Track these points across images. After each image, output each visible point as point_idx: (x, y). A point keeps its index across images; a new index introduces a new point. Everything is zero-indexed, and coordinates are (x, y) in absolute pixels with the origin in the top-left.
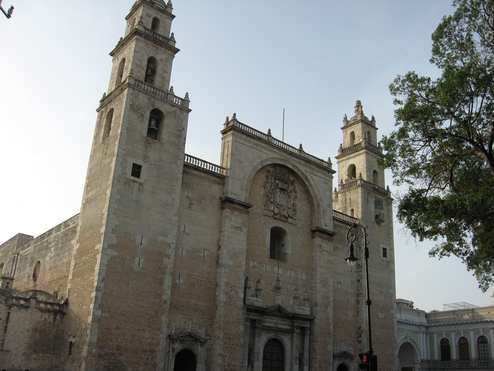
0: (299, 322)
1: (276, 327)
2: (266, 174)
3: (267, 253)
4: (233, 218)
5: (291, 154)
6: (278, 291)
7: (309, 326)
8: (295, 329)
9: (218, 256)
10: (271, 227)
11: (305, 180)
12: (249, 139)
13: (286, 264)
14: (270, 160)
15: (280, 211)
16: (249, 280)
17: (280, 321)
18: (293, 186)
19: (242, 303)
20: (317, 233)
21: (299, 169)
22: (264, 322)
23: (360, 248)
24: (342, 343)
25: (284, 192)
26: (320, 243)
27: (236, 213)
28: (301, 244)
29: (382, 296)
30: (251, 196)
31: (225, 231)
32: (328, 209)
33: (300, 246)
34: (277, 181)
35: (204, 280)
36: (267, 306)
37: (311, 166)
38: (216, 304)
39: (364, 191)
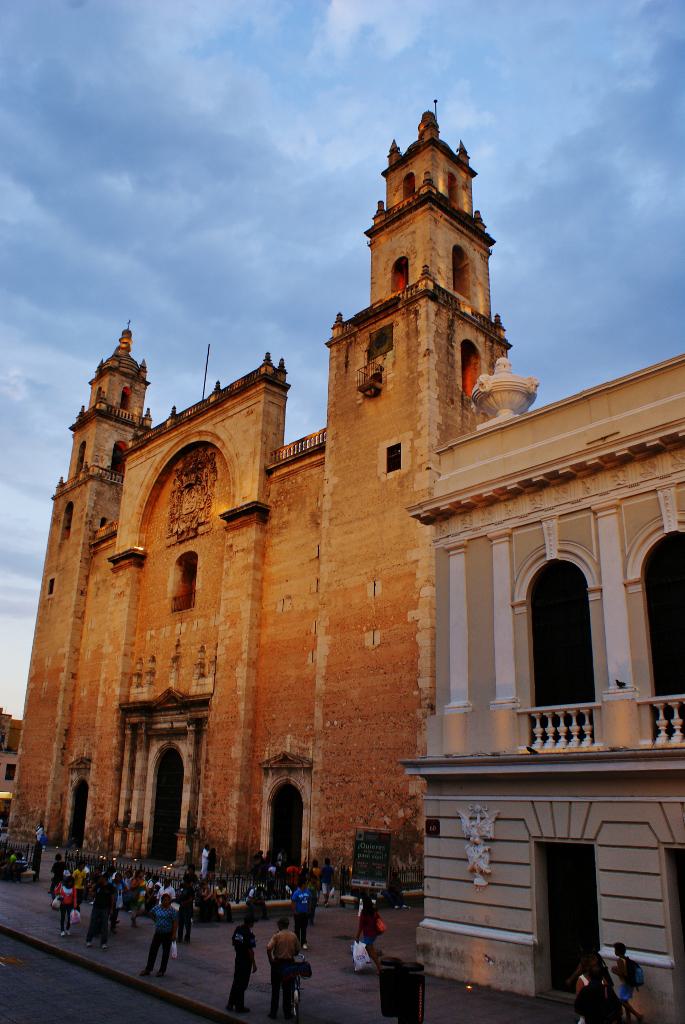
21: (206, 433)
24: (289, 736)
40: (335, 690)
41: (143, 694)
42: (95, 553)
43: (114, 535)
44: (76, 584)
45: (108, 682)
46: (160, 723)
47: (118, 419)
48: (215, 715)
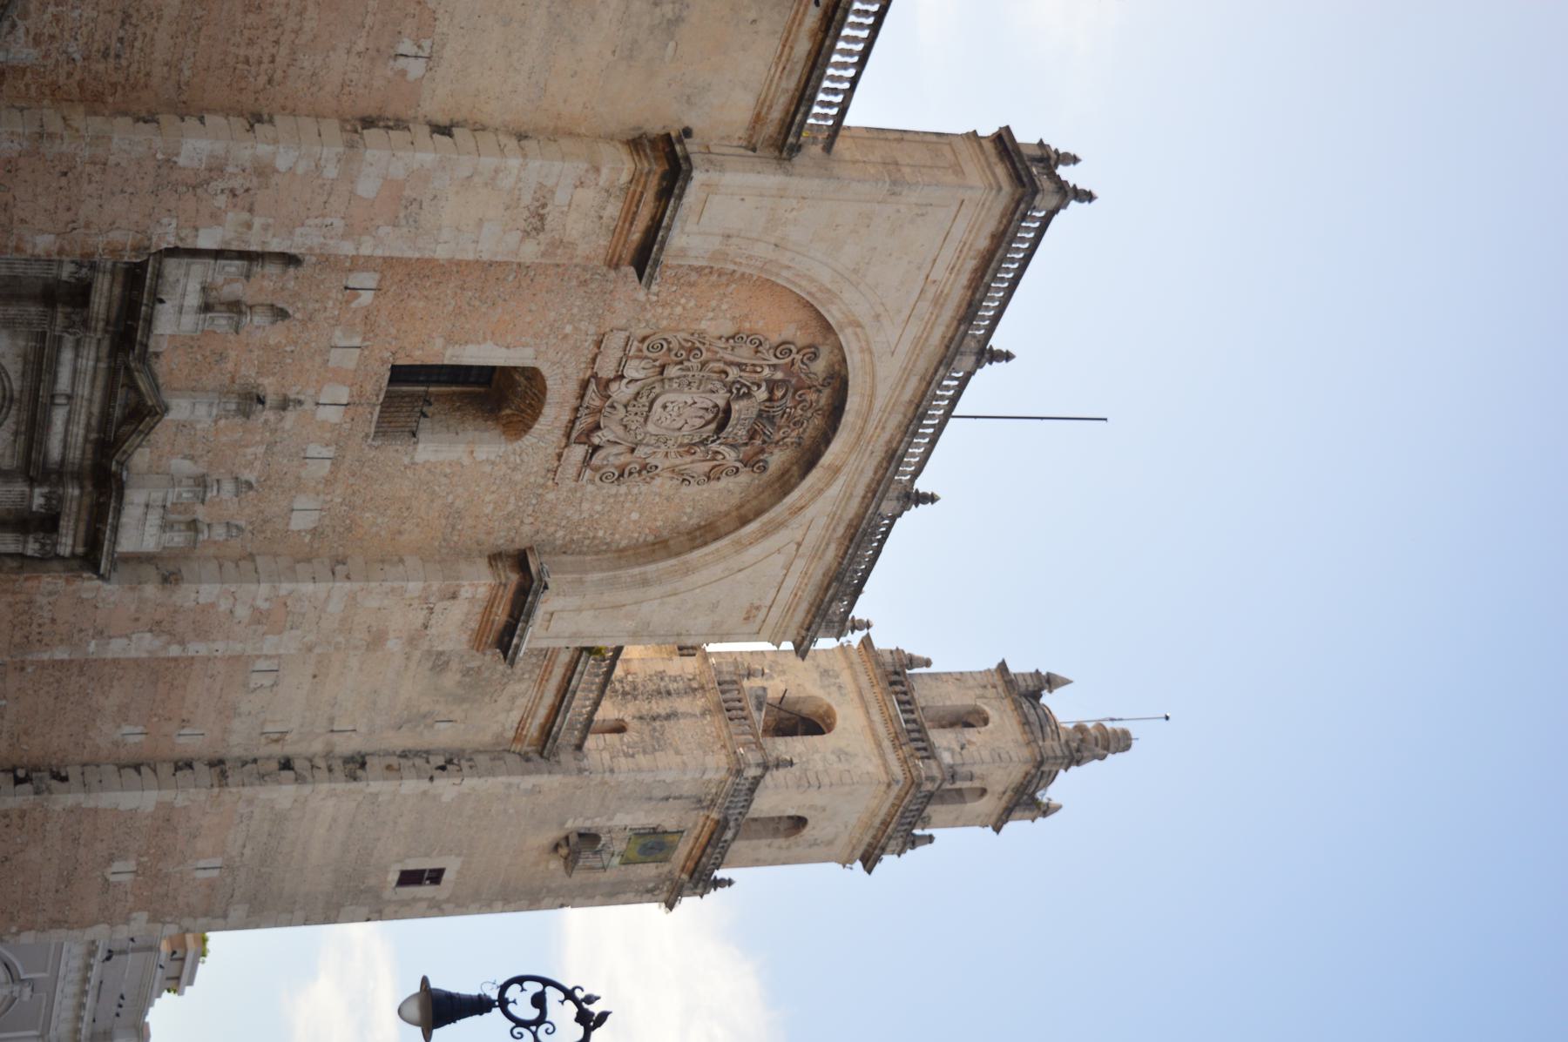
0: (80, 506)
1: (53, 397)
2: (800, 343)
3: (418, 353)
4: (587, 197)
5: (893, 458)
6: (233, 407)
7: (65, 548)
8: (45, 490)
9: (400, 124)
10: (545, 370)
11: (765, 518)
12: (971, 264)
13: (367, 436)
14: (863, 360)
15: (620, 407)
16: (285, 272)
17: (83, 418)
18: (738, 464)
19: (170, 241)
20: (514, 578)
22: (78, 345)
23: (443, 768)
25: (713, 426)
26: (466, 592)
27: (613, 209)
28: (459, 503)
29: (215, 873)
30: (694, 277)
31: (525, 156)
32: (630, 625)
33: (450, 498)
34: (762, 394)
35: (278, 59)
36: (157, 355)
37: (833, 546)
38: (163, 118)
39: (710, 781)
40: (48, 827)
46: (77, 356)
48: (50, 594)
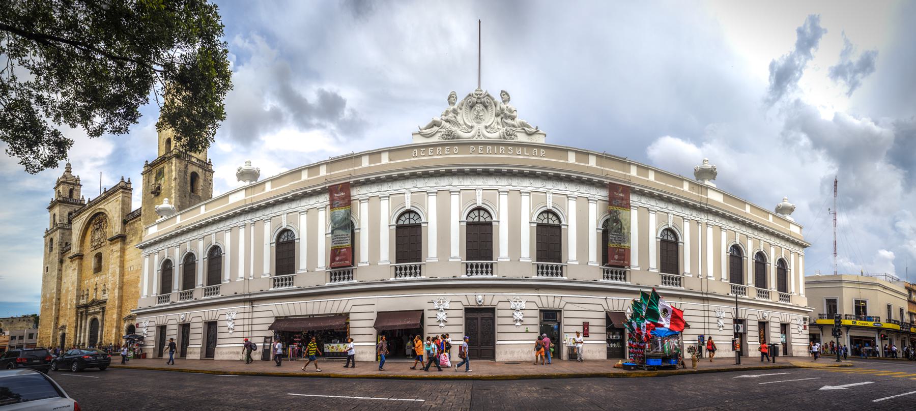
41: (83, 302)
42: (64, 256)
43: (70, 249)
44: (57, 268)
45: (71, 300)
47: (69, 203)
